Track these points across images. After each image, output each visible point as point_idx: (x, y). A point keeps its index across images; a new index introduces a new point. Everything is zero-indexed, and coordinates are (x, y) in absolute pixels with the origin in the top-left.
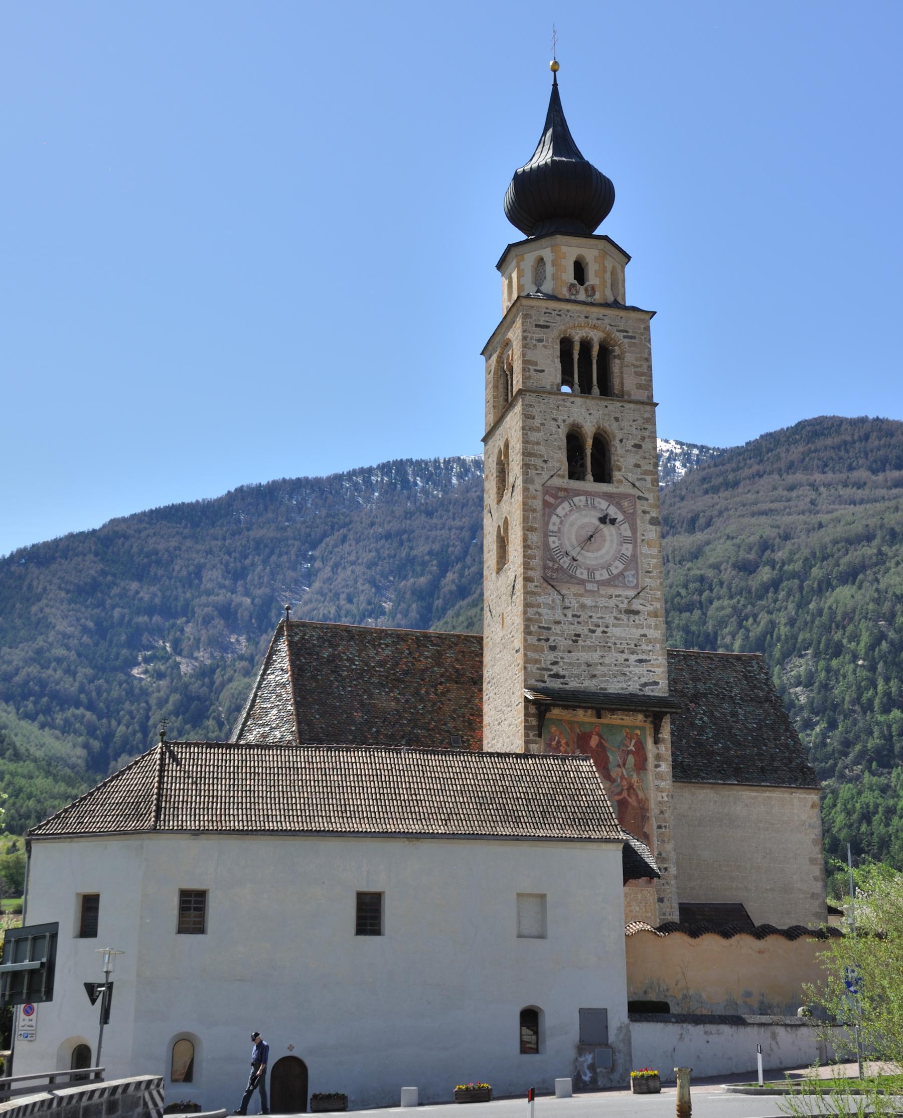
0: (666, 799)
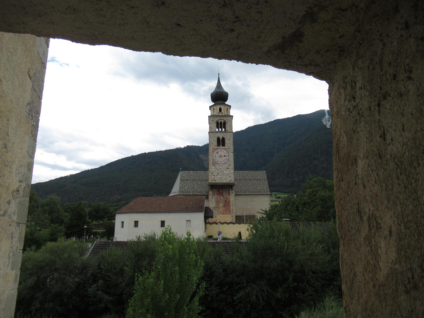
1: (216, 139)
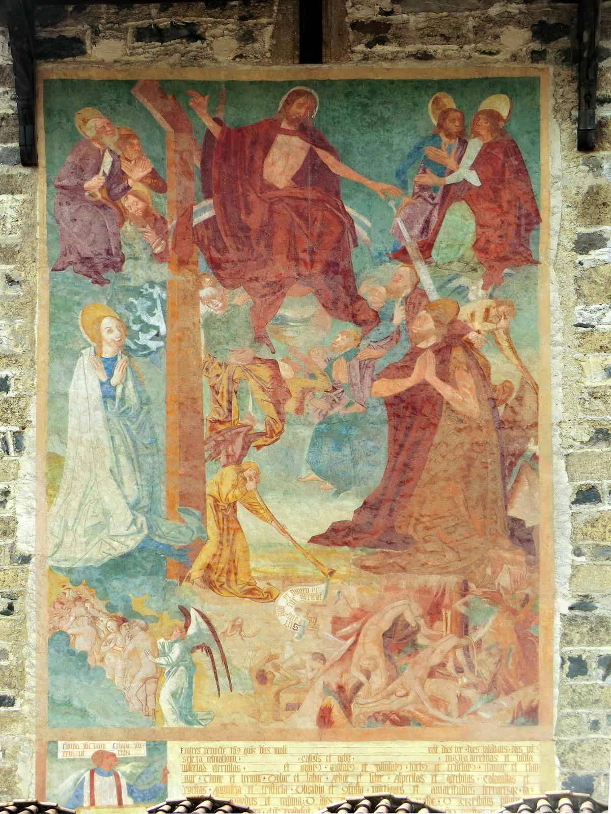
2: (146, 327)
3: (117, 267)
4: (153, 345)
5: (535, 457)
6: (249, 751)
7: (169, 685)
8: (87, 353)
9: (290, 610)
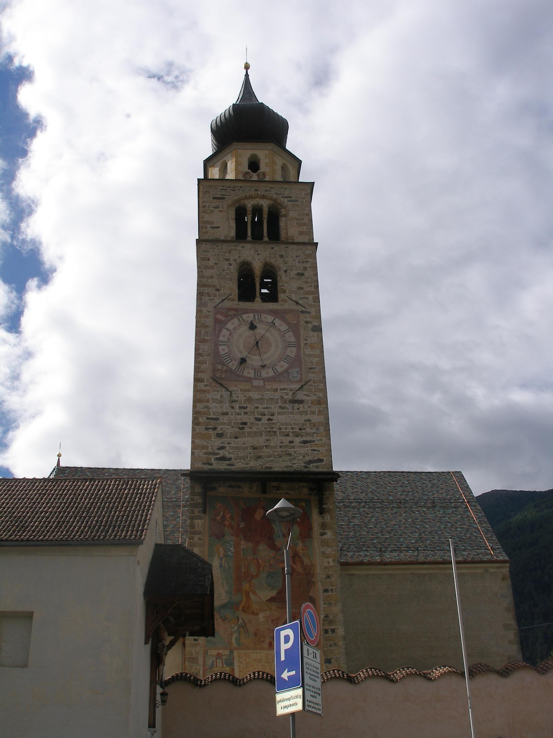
0: (332, 564)
1: (234, 271)
2: (230, 550)
3: (224, 536)
4: (231, 554)
5: (314, 582)
6: (253, 653)
7: (234, 636)
8: (217, 556)
9: (262, 617)
